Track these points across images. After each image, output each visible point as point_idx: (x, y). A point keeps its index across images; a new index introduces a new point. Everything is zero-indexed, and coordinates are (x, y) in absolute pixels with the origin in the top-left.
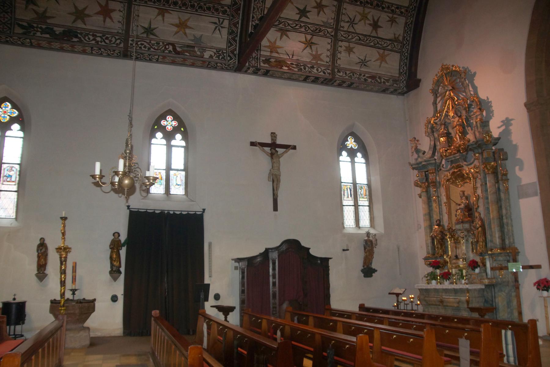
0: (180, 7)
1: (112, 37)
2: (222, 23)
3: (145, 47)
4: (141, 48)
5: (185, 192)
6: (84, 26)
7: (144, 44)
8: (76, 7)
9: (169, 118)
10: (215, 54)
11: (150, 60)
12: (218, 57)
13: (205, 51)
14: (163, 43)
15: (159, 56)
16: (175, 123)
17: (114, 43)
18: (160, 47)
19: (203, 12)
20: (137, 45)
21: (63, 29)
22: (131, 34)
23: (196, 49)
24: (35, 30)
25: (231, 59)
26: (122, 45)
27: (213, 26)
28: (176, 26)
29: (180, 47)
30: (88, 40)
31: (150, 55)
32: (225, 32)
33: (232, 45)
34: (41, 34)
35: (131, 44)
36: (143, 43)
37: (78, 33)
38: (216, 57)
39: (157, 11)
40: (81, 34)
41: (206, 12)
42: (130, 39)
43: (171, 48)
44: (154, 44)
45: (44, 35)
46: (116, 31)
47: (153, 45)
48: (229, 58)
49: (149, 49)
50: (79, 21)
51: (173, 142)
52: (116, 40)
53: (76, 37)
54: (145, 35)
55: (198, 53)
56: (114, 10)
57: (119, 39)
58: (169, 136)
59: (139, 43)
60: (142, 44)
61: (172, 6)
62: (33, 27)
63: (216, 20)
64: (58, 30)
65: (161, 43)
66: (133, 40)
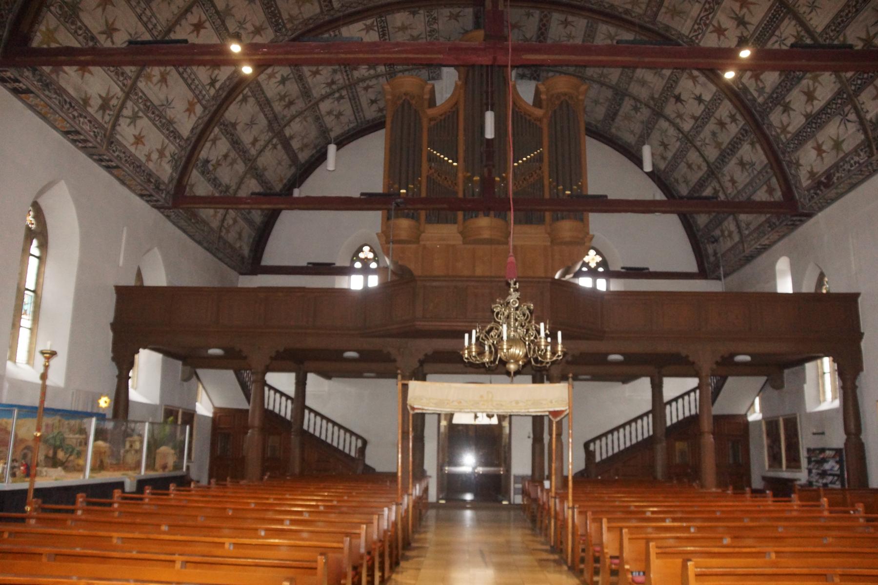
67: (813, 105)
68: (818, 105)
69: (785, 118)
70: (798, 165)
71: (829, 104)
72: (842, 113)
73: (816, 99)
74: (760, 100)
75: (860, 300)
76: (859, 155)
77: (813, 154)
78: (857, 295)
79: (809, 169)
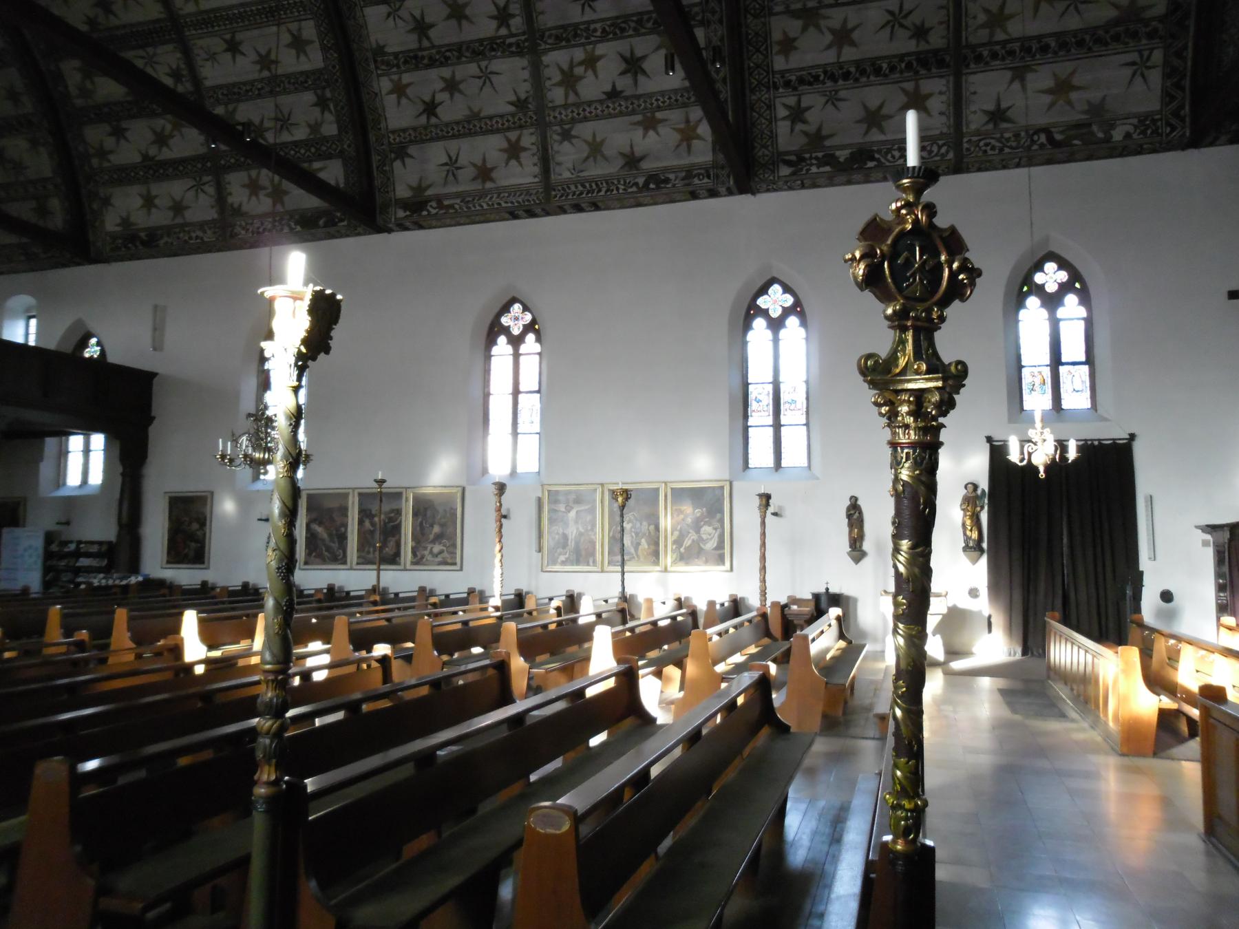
0: (1055, 53)
1: (932, 145)
2: (1149, 58)
3: (993, 148)
4: (985, 151)
5: (1092, 404)
6: (881, 137)
7: (990, 143)
8: (865, 107)
9: (1050, 267)
10: (1136, 127)
11: (1004, 167)
12: (1143, 132)
13: (1113, 127)
14: (1027, 132)
15: (1020, 160)
16: (1063, 276)
17: (936, 155)
18: (1022, 142)
19: (1103, 48)
20: (977, 149)
21: (850, 151)
22: (965, 130)
23: (1095, 128)
24: (808, 165)
25: (1173, 129)
26: (951, 155)
27: (1128, 71)
28: (1049, 91)
29: (1061, 132)
30: (891, 159)
31: (1003, 160)
32: (1155, 77)
33: (1173, 98)
34: (818, 168)
35: (968, 149)
36: (988, 141)
37: (873, 151)
38: (1138, 135)
39: (1009, 74)
40: (879, 151)
41: (1110, 47)
42: (965, 140)
43: (1043, 138)
44: (1010, 138)
45: (822, 169)
46: (937, 132)
47: (1008, 140)
48: (1168, 129)
49: (1001, 150)
50: (874, 130)
51: (1061, 313)
52: (940, 147)
53: (872, 159)
54: (991, 126)
55: (1101, 135)
56: (930, 95)
57: (944, 145)
58: (1052, 301)
59: (982, 144)
60: (987, 145)
61: (1038, 56)
62: (803, 160)
63: (1134, 57)
64: (842, 155)
65: (1023, 134)
66: (970, 140)
67: (160, 150)
68: (166, 154)
69: (110, 142)
70: (106, 202)
71: (183, 161)
72: (198, 179)
73: (168, 146)
74: (79, 102)
75: (155, 381)
76: (205, 232)
77: (139, 202)
78: (153, 375)
79: (124, 214)
